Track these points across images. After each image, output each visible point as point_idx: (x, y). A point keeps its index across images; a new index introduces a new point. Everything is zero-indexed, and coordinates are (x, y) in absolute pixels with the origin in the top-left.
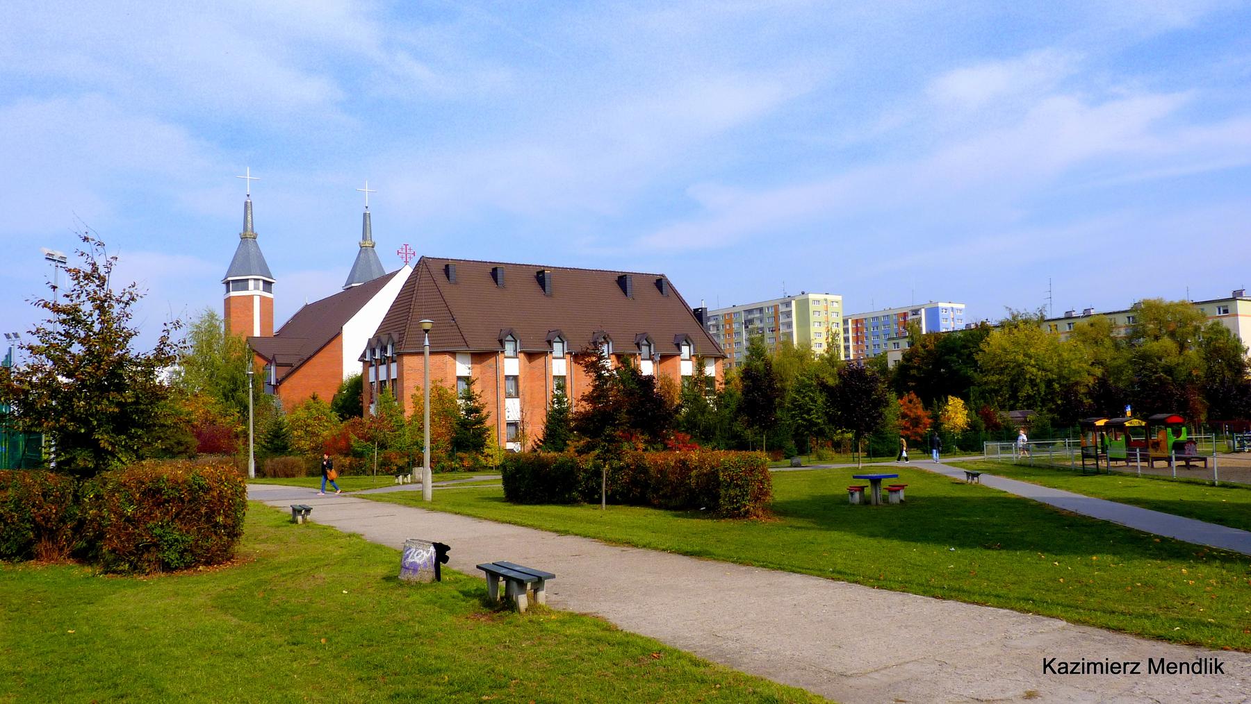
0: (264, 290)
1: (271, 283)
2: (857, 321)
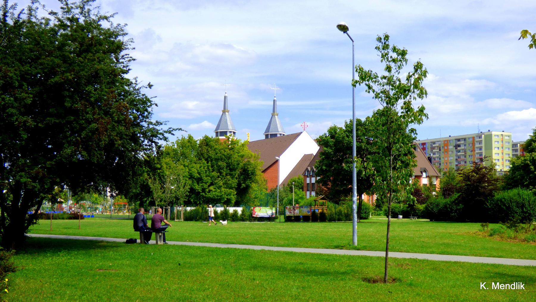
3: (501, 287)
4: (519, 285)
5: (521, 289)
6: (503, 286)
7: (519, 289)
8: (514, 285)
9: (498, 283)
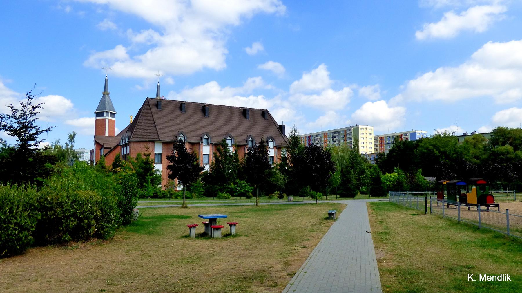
0: (111, 116)
1: (115, 114)
2: (381, 138)
3: (488, 278)
4: (505, 276)
5: (507, 280)
6: (489, 277)
8: (501, 277)
9: (485, 275)
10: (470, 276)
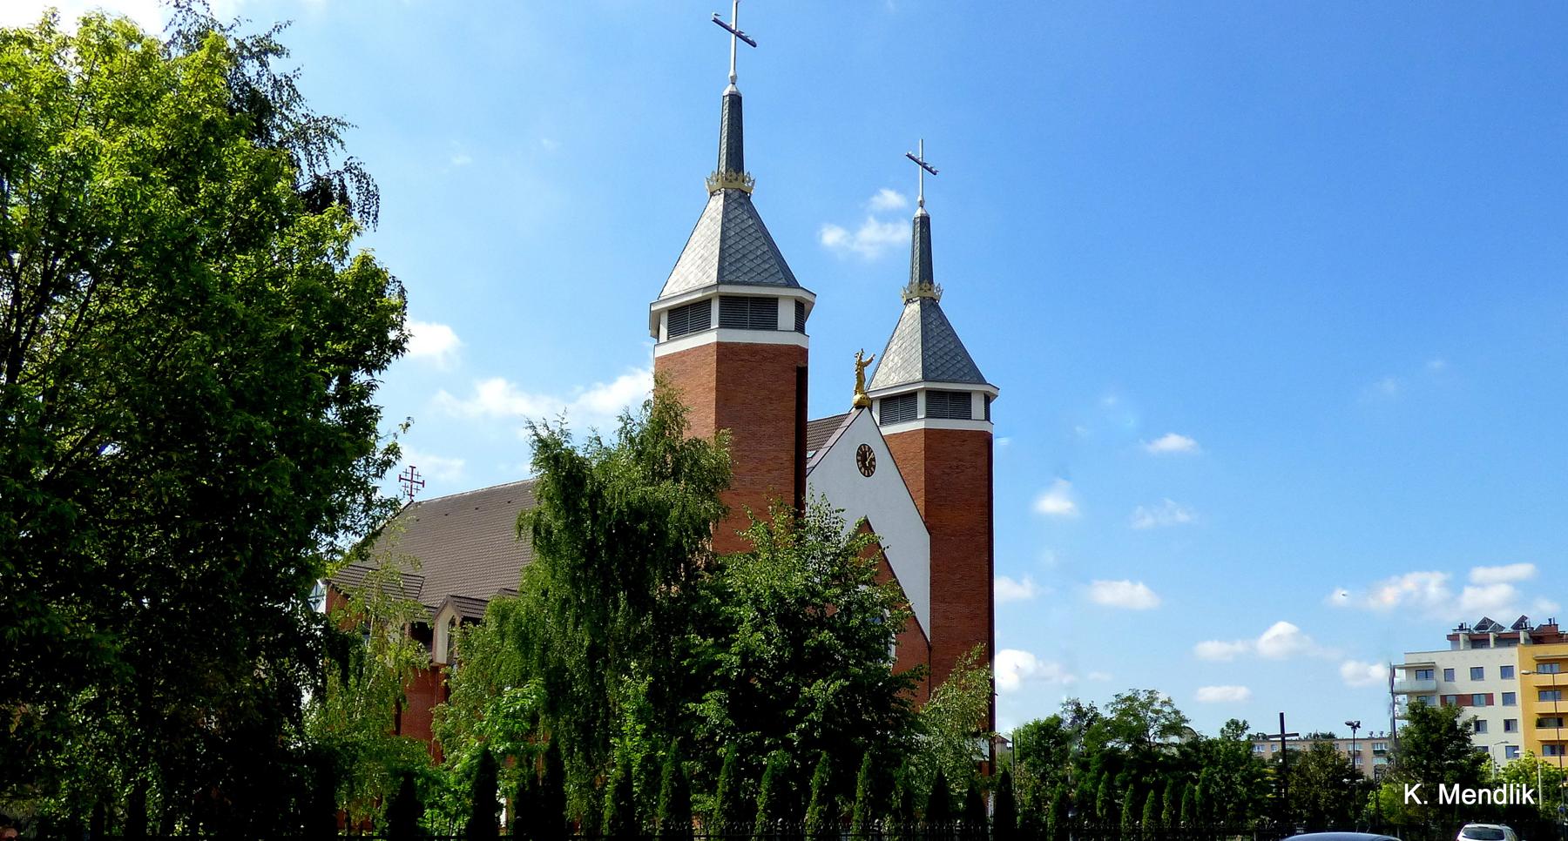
3: (1464, 796)
5: (1524, 802)
6: (1469, 793)
7: (1518, 802)
8: (1504, 791)
9: (1457, 787)
10: (1409, 790)
